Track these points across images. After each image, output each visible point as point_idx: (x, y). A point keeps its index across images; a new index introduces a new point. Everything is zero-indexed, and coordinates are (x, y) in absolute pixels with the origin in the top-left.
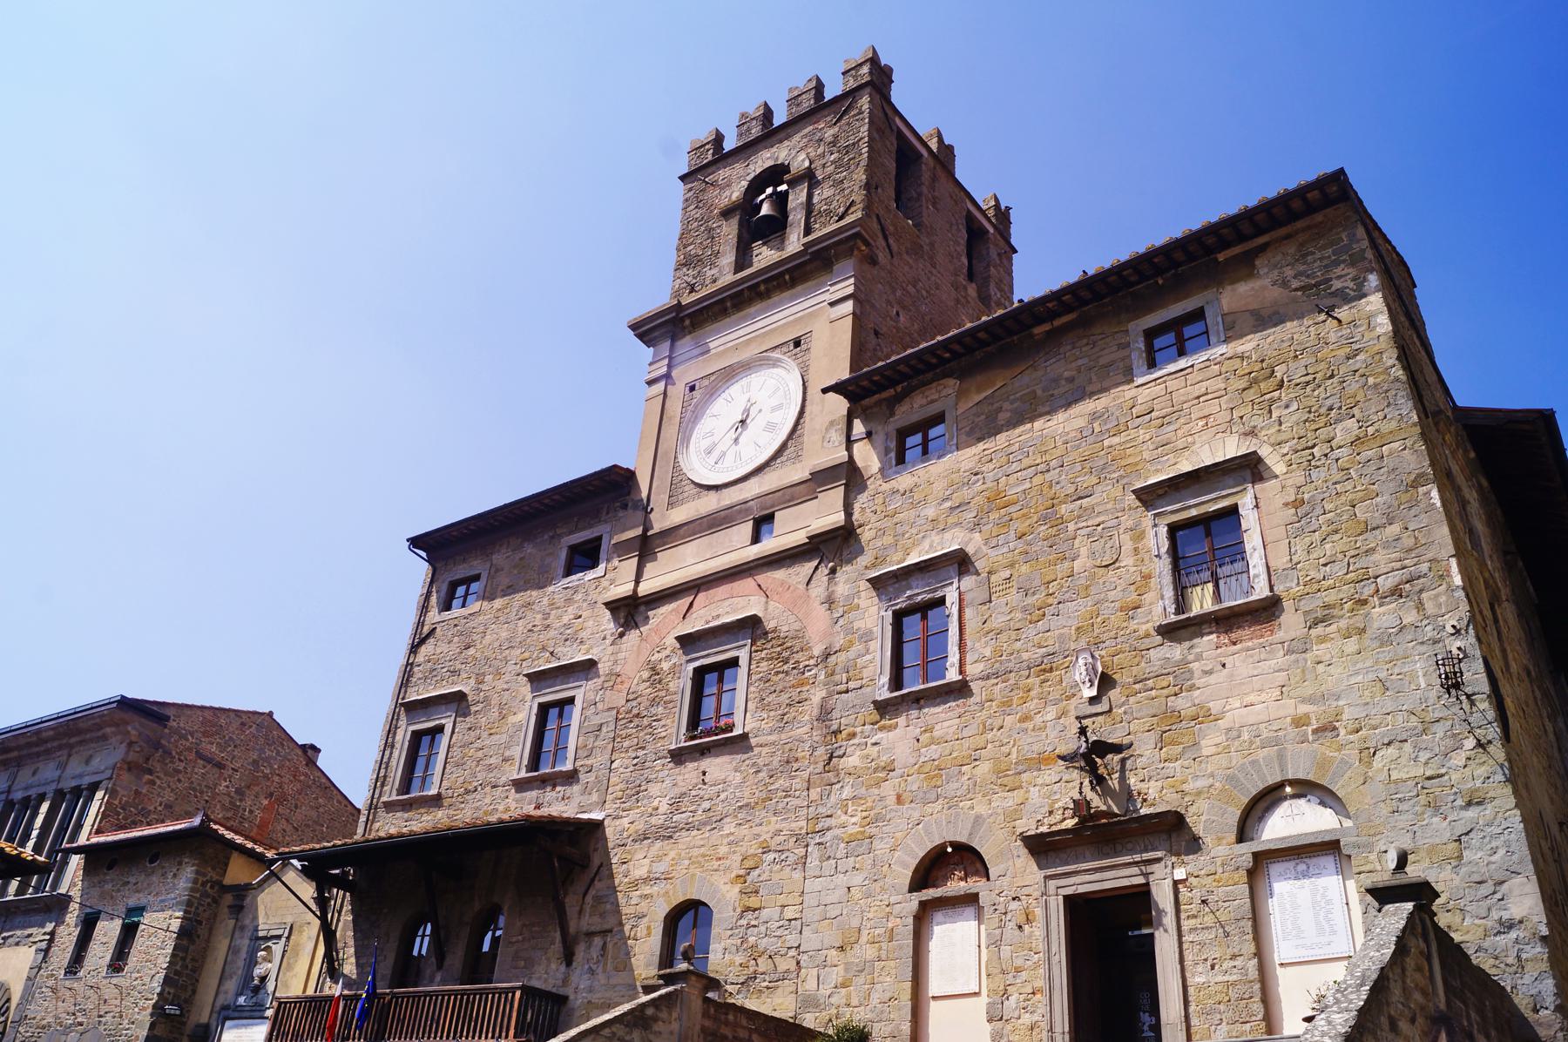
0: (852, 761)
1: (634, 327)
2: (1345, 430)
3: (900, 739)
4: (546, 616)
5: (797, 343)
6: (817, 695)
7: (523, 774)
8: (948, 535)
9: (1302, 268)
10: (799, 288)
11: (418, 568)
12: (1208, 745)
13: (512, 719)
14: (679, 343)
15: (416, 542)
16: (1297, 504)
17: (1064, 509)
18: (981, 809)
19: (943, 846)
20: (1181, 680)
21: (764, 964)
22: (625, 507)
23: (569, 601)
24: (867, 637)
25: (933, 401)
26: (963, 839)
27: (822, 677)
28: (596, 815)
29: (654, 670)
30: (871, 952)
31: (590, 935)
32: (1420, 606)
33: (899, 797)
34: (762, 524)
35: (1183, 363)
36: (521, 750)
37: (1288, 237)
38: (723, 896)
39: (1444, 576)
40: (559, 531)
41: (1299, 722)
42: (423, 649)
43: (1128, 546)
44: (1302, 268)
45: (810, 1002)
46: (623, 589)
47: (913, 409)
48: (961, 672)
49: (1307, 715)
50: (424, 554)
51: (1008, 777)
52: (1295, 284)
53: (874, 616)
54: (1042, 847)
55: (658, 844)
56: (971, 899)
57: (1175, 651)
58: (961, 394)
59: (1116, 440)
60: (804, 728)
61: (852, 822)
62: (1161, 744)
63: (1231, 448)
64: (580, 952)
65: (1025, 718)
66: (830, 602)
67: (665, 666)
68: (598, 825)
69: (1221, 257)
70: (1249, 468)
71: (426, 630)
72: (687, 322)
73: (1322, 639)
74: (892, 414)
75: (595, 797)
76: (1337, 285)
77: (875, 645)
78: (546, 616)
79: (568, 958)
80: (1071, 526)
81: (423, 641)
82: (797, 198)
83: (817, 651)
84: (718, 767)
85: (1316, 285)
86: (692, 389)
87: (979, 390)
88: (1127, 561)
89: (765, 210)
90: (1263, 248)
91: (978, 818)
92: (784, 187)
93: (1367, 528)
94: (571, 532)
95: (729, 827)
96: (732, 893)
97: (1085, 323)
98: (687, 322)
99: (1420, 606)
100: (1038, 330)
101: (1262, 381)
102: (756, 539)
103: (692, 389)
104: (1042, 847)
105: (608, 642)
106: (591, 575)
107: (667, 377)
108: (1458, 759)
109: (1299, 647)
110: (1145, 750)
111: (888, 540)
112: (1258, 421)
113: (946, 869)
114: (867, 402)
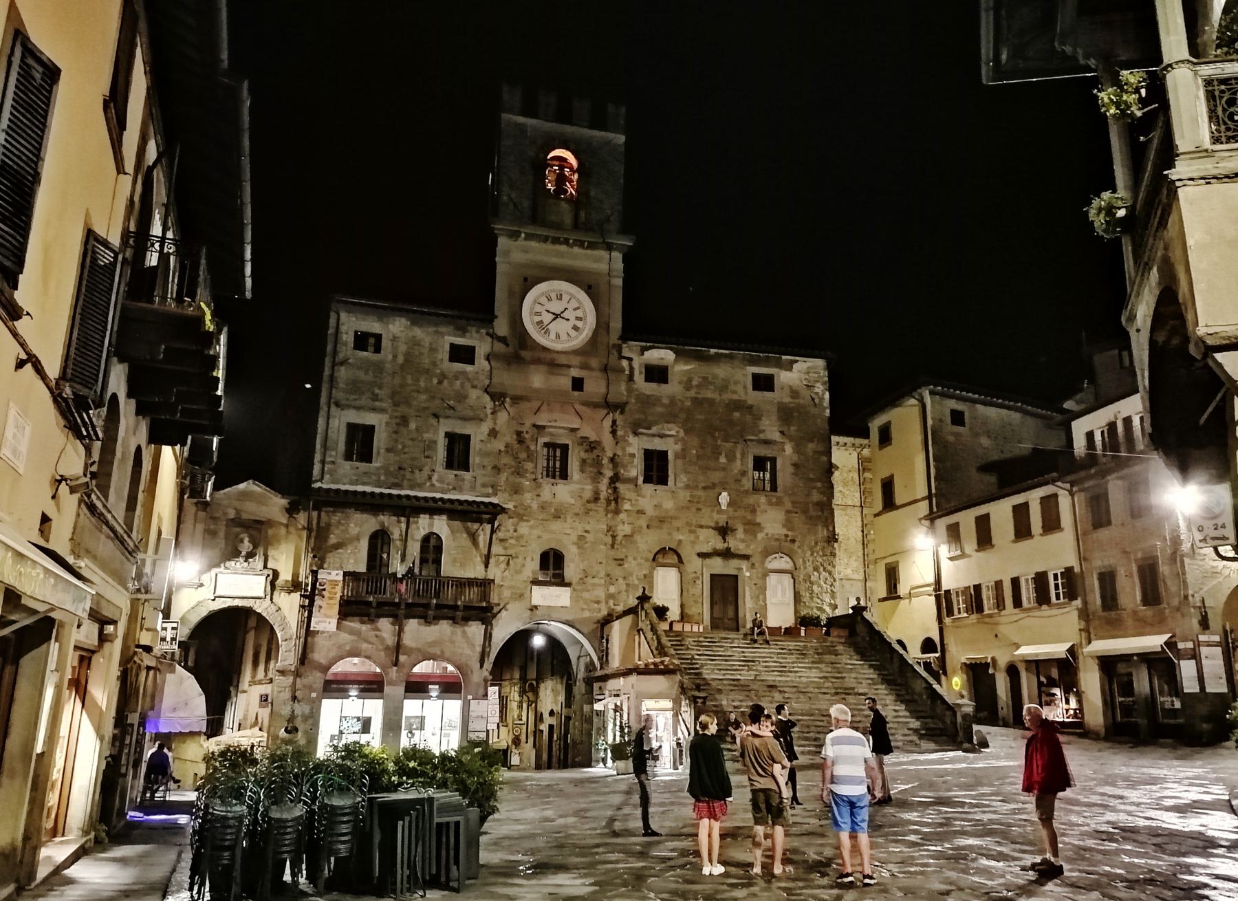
0: (627, 506)
2: (811, 446)
4: (440, 382)
6: (609, 473)
8: (670, 425)
10: (589, 252)
13: (426, 436)
18: (681, 537)
20: (754, 511)
21: (589, 580)
22: (488, 334)
23: (456, 377)
24: (633, 455)
27: (611, 466)
29: (519, 434)
30: (636, 582)
40: (442, 329)
41: (787, 536)
42: (343, 368)
43: (738, 456)
51: (694, 528)
54: (700, 555)
55: (532, 522)
57: (752, 499)
59: (737, 414)
60: (604, 486)
61: (627, 529)
62: (745, 531)
63: (776, 436)
65: (699, 509)
66: (614, 432)
67: (527, 436)
75: (490, 490)
76: (816, 390)
77: (636, 460)
78: (440, 382)
79: (486, 566)
83: (610, 454)
87: (686, 363)
88: (738, 463)
91: (680, 541)
93: (812, 480)
95: (569, 520)
96: (574, 549)
104: (700, 555)
106: (469, 368)
109: (788, 512)
110: (740, 534)
111: (642, 417)
112: (785, 429)
113: (668, 555)
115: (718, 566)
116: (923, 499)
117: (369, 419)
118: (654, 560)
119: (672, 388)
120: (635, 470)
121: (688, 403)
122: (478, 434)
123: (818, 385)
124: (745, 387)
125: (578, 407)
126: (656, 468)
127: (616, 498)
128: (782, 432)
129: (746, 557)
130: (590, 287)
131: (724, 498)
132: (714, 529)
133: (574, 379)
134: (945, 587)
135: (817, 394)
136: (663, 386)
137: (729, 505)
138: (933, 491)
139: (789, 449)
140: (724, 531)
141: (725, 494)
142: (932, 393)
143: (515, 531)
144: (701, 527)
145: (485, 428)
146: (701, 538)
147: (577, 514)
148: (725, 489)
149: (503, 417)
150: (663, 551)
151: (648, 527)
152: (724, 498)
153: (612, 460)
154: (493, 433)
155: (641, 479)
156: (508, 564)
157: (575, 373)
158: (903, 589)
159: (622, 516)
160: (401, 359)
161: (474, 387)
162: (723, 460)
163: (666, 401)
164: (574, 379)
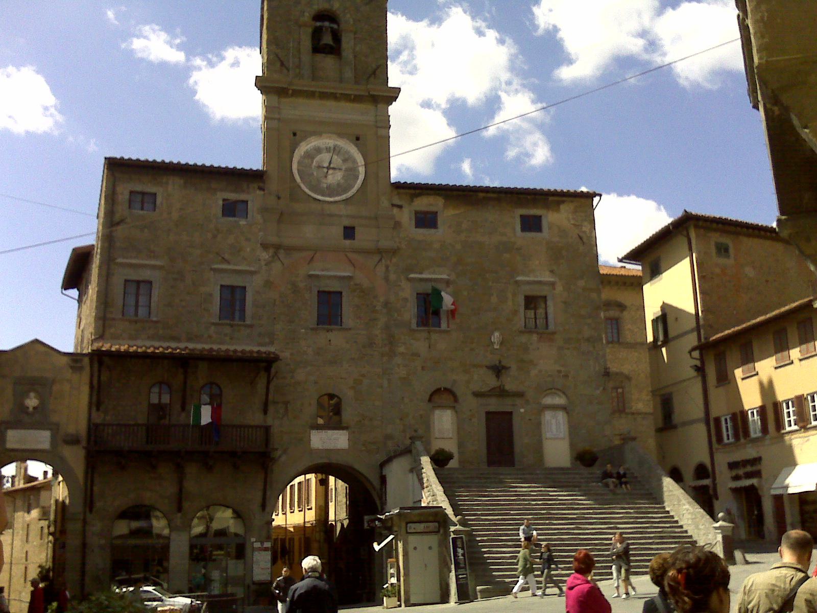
0: (402, 349)
2: (581, 283)
3: (420, 345)
4: (215, 237)
5: (358, 139)
6: (382, 320)
7: (217, 321)
9: (575, 216)
12: (534, 372)
14: (283, 100)
16: (565, 303)
17: (487, 275)
19: (441, 389)
22: (261, 189)
24: (406, 300)
25: (431, 205)
26: (449, 386)
28: (272, 349)
31: (275, 403)
32: (594, 347)
33: (422, 367)
34: (349, 232)
35: (533, 234)
36: (215, 306)
37: (572, 202)
38: (347, 394)
39: (601, 339)
41: (559, 372)
44: (575, 216)
45: (388, 437)
46: (273, 239)
47: (423, 203)
48: (448, 327)
49: (561, 370)
52: (572, 222)
53: (408, 292)
54: (477, 395)
56: (454, 408)
57: (524, 339)
58: (445, 206)
59: (507, 256)
63: (547, 277)
64: (271, 408)
65: (472, 350)
66: (387, 279)
67: (301, 285)
69: (551, 198)
70: (553, 284)
71: (117, 217)
72: (290, 92)
73: (568, 349)
74: (412, 201)
75: (267, 340)
76: (584, 229)
78: (215, 237)
79: (265, 412)
80: (490, 284)
81: (118, 224)
82: (347, 43)
83: (382, 299)
84: (336, 339)
85: (578, 225)
86: (295, 134)
88: (510, 303)
89: (327, 39)
90: (563, 202)
91: (455, 381)
92: (335, 26)
94: (222, 190)
96: (351, 393)
97: (498, 200)
98: (290, 92)
99: (594, 347)
100: (481, 195)
101: (556, 254)
103: (295, 134)
104: (477, 395)
105: (263, 263)
106: (243, 222)
107: (279, 119)
108: (598, 392)
113: (443, 395)
114: (402, 191)
115: (494, 405)
116: (692, 331)
117: (145, 275)
118: (430, 400)
119: (441, 234)
120: (410, 313)
121: (458, 247)
122: (253, 285)
123: (586, 223)
124: (514, 229)
125: (350, 255)
126: (429, 308)
127: (391, 341)
128: (552, 271)
129: (520, 395)
130: (358, 139)
131: (496, 337)
132: (488, 367)
133: (346, 228)
134: (714, 414)
135: (585, 232)
136: (433, 231)
137: (502, 344)
138: (701, 322)
139: (559, 288)
140: (498, 370)
141: (497, 334)
142: (696, 227)
143: (292, 377)
144: (475, 366)
146: (476, 377)
147: (353, 359)
148: (496, 329)
149: (277, 267)
150: (437, 391)
151: (423, 368)
152: (496, 337)
153: (386, 304)
154: (268, 284)
155: (414, 321)
156: (286, 410)
157: (347, 223)
158: (677, 418)
159: (398, 360)
160: (175, 215)
161: (248, 240)
162: (494, 299)
163: (436, 246)
164: (346, 228)
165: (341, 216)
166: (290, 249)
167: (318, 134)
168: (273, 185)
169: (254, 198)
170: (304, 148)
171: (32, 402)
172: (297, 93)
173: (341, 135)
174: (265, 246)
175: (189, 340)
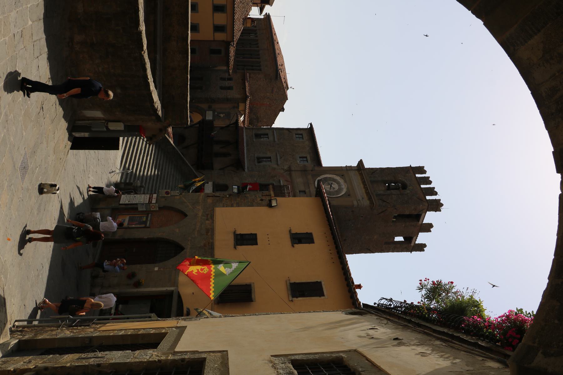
1: (361, 160)
5: (349, 195)
11: (305, 126)
15: (311, 124)
28: (246, 170)
36: (261, 155)
50: (309, 126)
68: (244, 170)
79: (220, 169)
102: (300, 191)
130: (349, 195)
145: (275, 166)
157: (307, 191)
165: (309, 188)
166: (290, 175)
167: (345, 182)
168: (317, 168)
169: (309, 164)
170: (338, 178)
171: (222, 115)
172: (361, 174)
173: (348, 188)
174: (290, 167)
175: (247, 149)
